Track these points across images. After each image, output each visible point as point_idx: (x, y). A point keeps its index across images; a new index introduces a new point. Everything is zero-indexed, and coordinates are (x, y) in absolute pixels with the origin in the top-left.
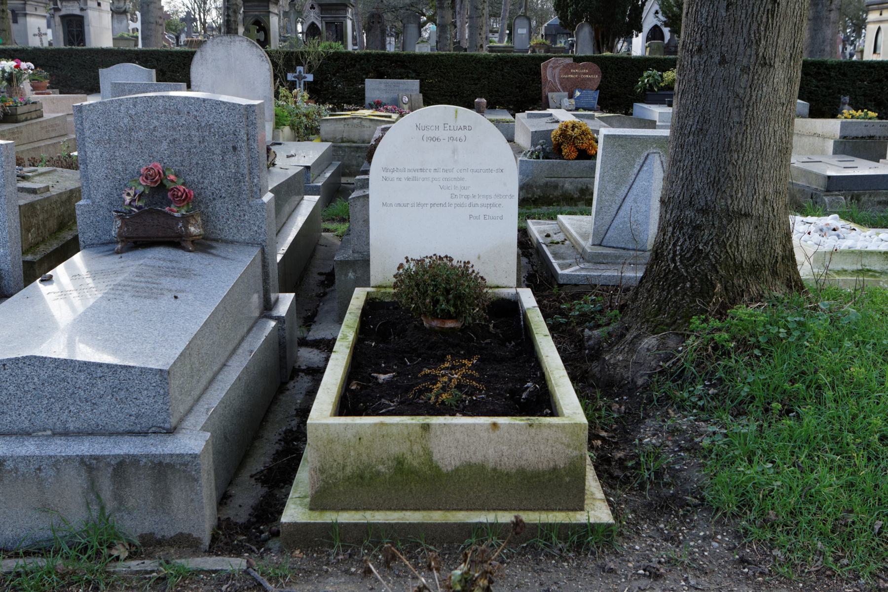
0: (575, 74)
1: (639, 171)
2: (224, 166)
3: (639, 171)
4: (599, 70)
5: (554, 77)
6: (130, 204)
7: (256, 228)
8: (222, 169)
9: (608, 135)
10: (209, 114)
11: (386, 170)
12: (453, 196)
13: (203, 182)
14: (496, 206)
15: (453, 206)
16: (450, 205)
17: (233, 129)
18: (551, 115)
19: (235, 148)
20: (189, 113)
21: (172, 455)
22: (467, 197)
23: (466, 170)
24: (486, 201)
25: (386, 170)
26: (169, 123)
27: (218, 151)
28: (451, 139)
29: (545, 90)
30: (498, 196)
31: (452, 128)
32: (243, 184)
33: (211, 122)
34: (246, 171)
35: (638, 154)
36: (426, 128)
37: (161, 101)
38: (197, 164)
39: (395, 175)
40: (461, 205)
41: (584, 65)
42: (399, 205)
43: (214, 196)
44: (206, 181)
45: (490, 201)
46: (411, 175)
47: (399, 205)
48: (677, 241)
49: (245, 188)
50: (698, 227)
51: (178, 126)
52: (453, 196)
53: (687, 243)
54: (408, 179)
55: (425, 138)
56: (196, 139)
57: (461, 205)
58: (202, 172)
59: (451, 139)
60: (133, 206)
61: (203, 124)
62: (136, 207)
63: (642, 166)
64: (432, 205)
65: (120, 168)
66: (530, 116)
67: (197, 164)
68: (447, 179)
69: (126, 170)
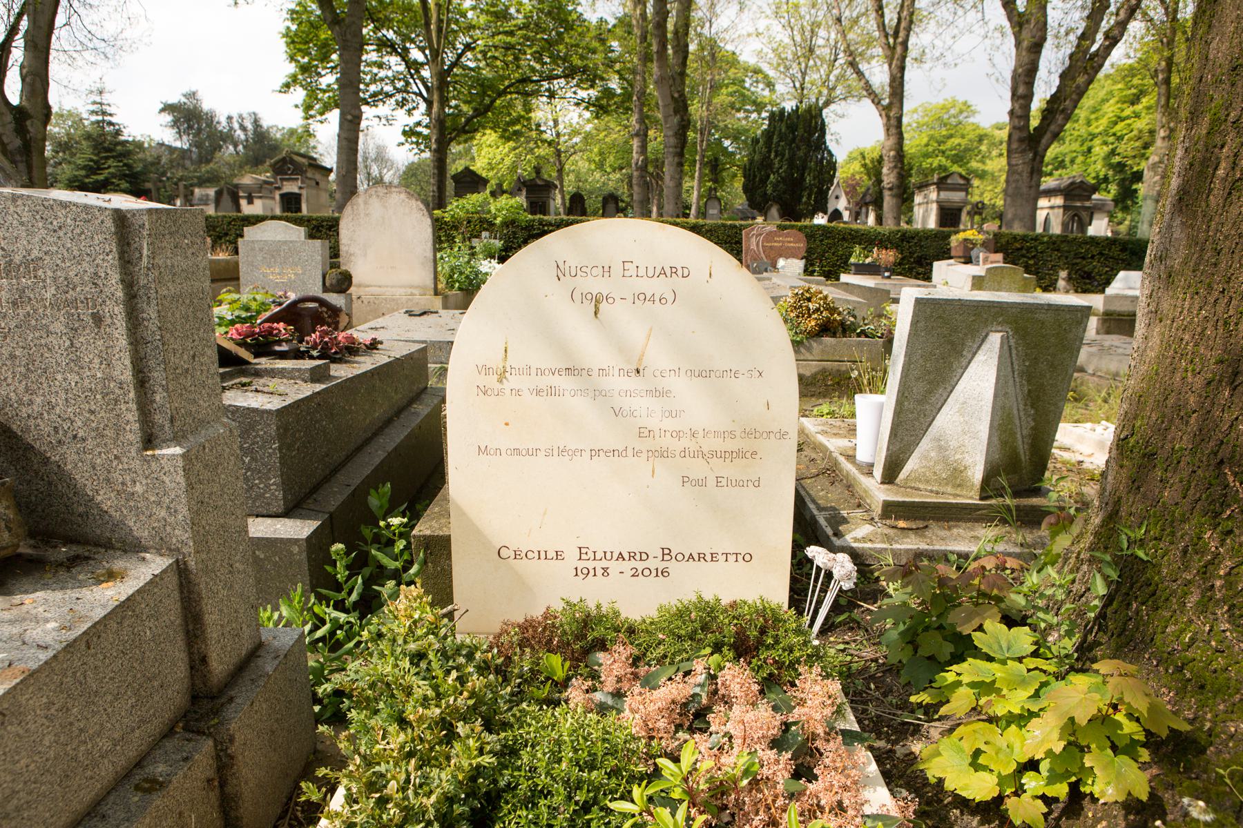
0: (779, 242)
5: (758, 245)
7: (163, 513)
8: (72, 371)
10: (30, 233)
13: (31, 403)
14: (744, 457)
15: (644, 455)
16: (636, 453)
19: (98, 319)
27: (58, 327)
28: (642, 297)
31: (642, 272)
32: (123, 407)
33: (35, 253)
34: (128, 376)
38: (12, 357)
42: (517, 451)
47: (517, 451)
54: (538, 392)
55: (577, 296)
58: (26, 377)
59: (642, 297)
61: (17, 259)
63: (975, 354)
67: (12, 357)
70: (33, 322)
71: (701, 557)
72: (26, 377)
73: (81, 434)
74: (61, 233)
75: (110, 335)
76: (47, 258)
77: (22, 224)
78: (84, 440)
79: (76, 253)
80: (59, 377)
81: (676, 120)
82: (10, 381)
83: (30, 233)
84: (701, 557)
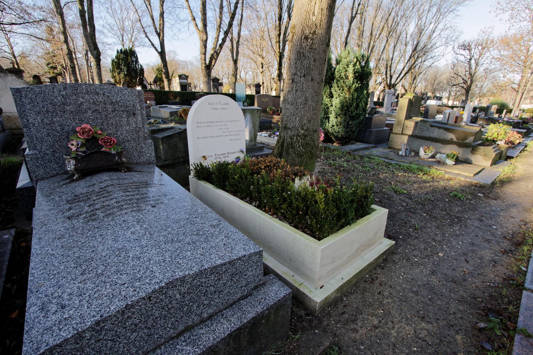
2: (129, 124)
6: (76, 151)
8: (127, 126)
11: (198, 123)
12: (224, 132)
13: (117, 134)
16: (223, 136)
17: (132, 103)
18: (167, 107)
19: (134, 114)
20: (104, 94)
22: (229, 132)
23: (228, 121)
24: (235, 133)
25: (198, 123)
26: (91, 100)
27: (124, 116)
28: (223, 108)
30: (239, 131)
33: (119, 100)
34: (141, 126)
36: (213, 104)
37: (84, 86)
38: (112, 123)
39: (202, 125)
40: (227, 136)
45: (236, 133)
46: (208, 124)
48: (299, 141)
49: (142, 135)
50: (306, 136)
51: (98, 102)
52: (224, 132)
53: (303, 141)
54: (207, 126)
56: (110, 110)
57: (227, 136)
59: (223, 108)
60: (78, 152)
61: (114, 101)
62: (81, 152)
64: (217, 136)
65: (59, 129)
66: (160, 107)
68: (221, 125)
69: (63, 129)
71: (233, 153)
72: (116, 128)
75: (137, 118)
76: (122, 101)
78: (130, 141)
80: (124, 127)
81: (95, 52)
84: (233, 153)
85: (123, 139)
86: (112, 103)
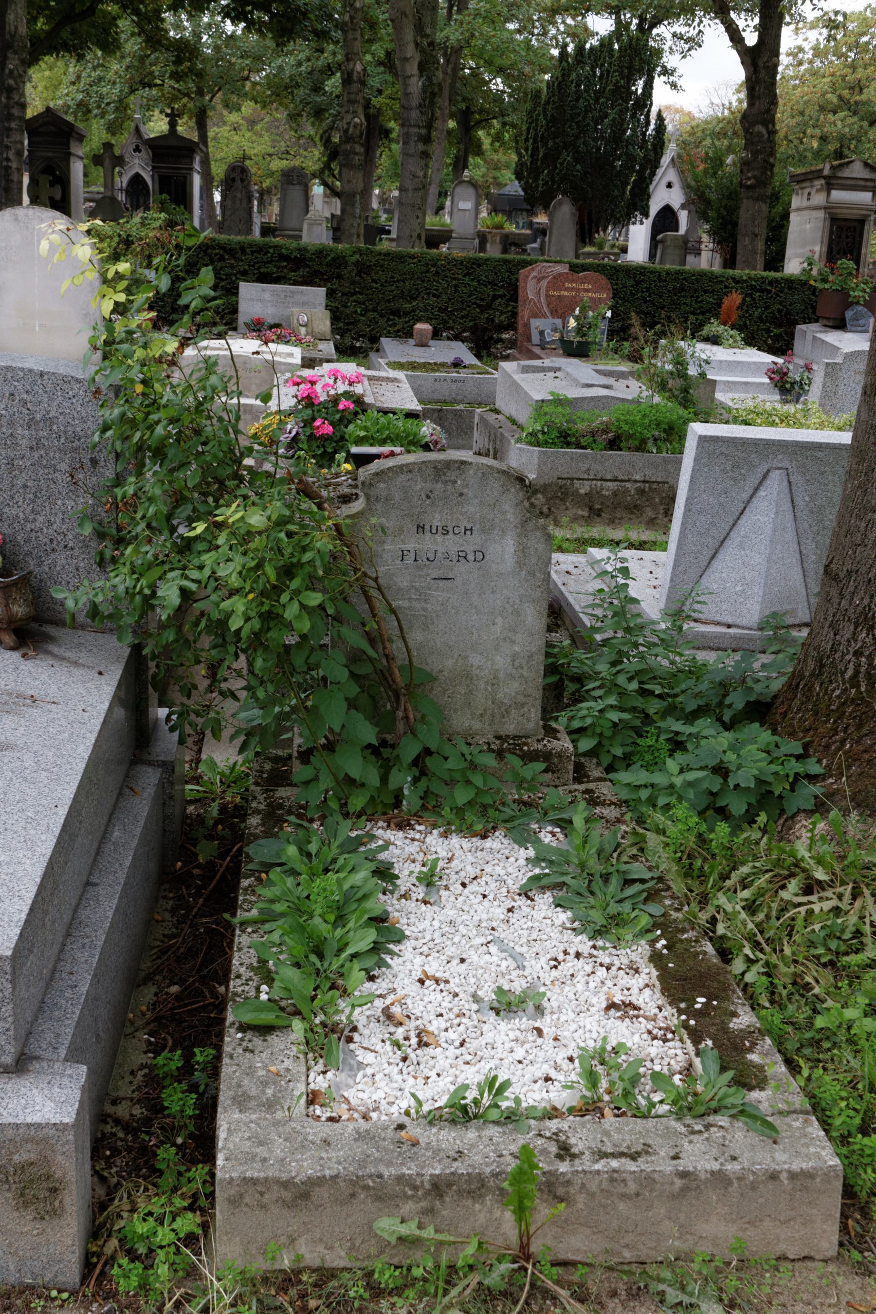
1: (751, 497)
3: (751, 497)
4: (609, 286)
8: (70, 498)
9: (705, 437)
10: (51, 400)
20: (12, 395)
21: (17, 1126)
27: (64, 467)
29: (524, 313)
33: (53, 414)
35: (752, 467)
38: (25, 486)
41: (585, 277)
43: (54, 545)
44: (41, 519)
56: (24, 442)
58: (33, 501)
61: (38, 417)
63: (756, 490)
66: (525, 370)
67: (25, 486)
70: (45, 462)
72: (33, 501)
73: (71, 544)
74: (74, 401)
76: (61, 417)
77: (46, 392)
79: (84, 415)
80: (59, 502)
82: (20, 504)
83: (51, 400)
85: (51, 541)
86: (31, 423)
